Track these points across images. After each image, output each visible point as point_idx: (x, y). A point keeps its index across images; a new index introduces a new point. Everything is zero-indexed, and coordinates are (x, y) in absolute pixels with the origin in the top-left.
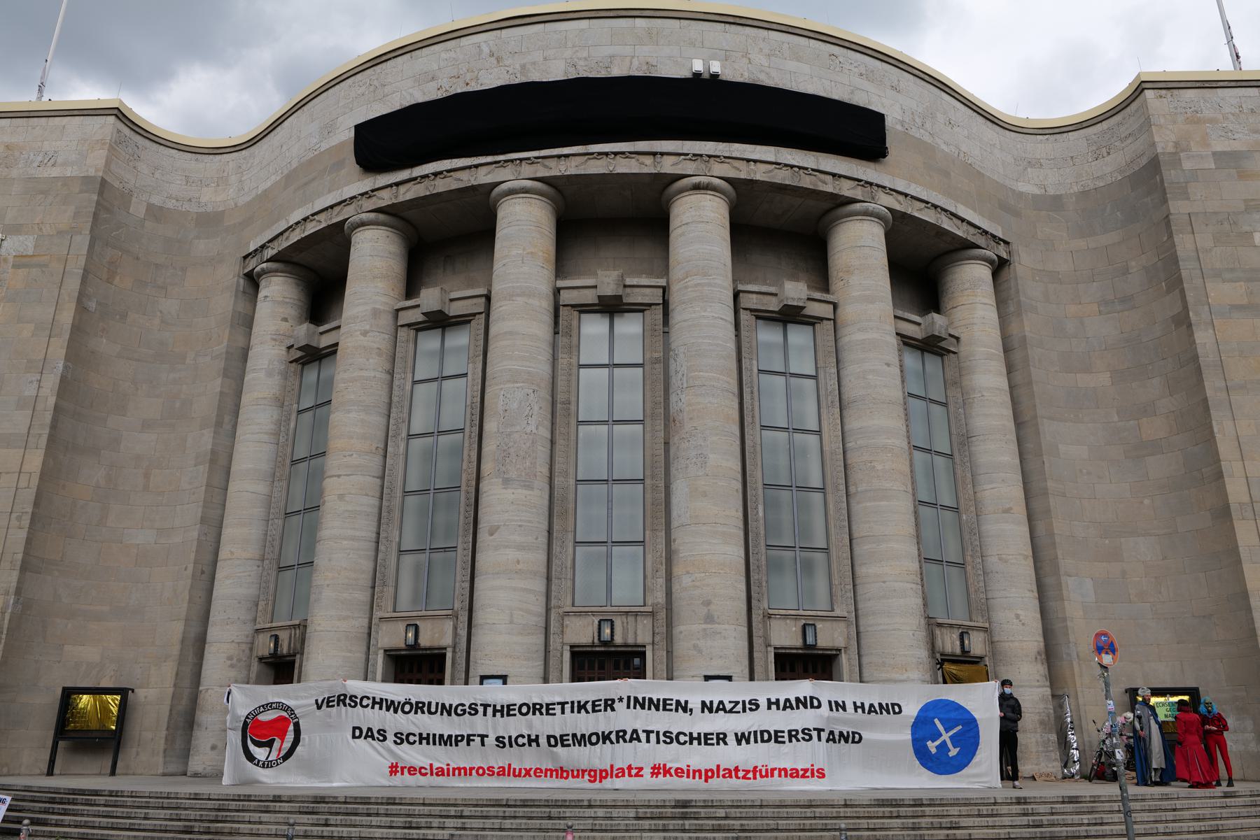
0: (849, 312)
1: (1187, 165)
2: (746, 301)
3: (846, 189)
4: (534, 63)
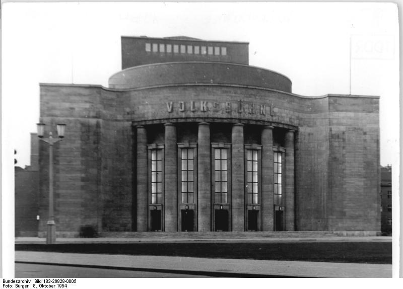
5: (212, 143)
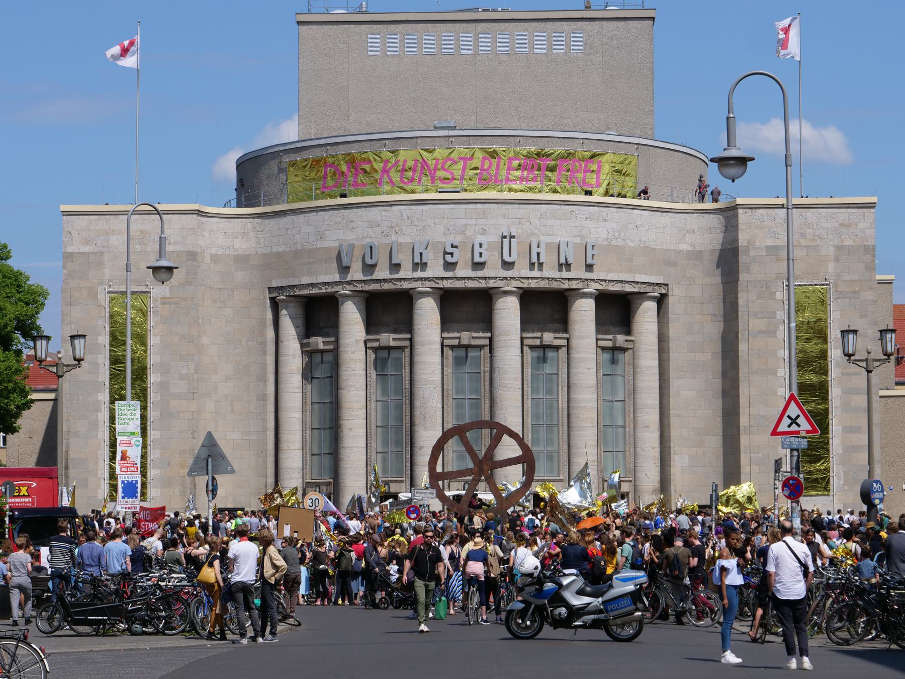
0: (574, 342)
1: (752, 253)
2: (526, 342)
3: (574, 285)
4: (429, 226)
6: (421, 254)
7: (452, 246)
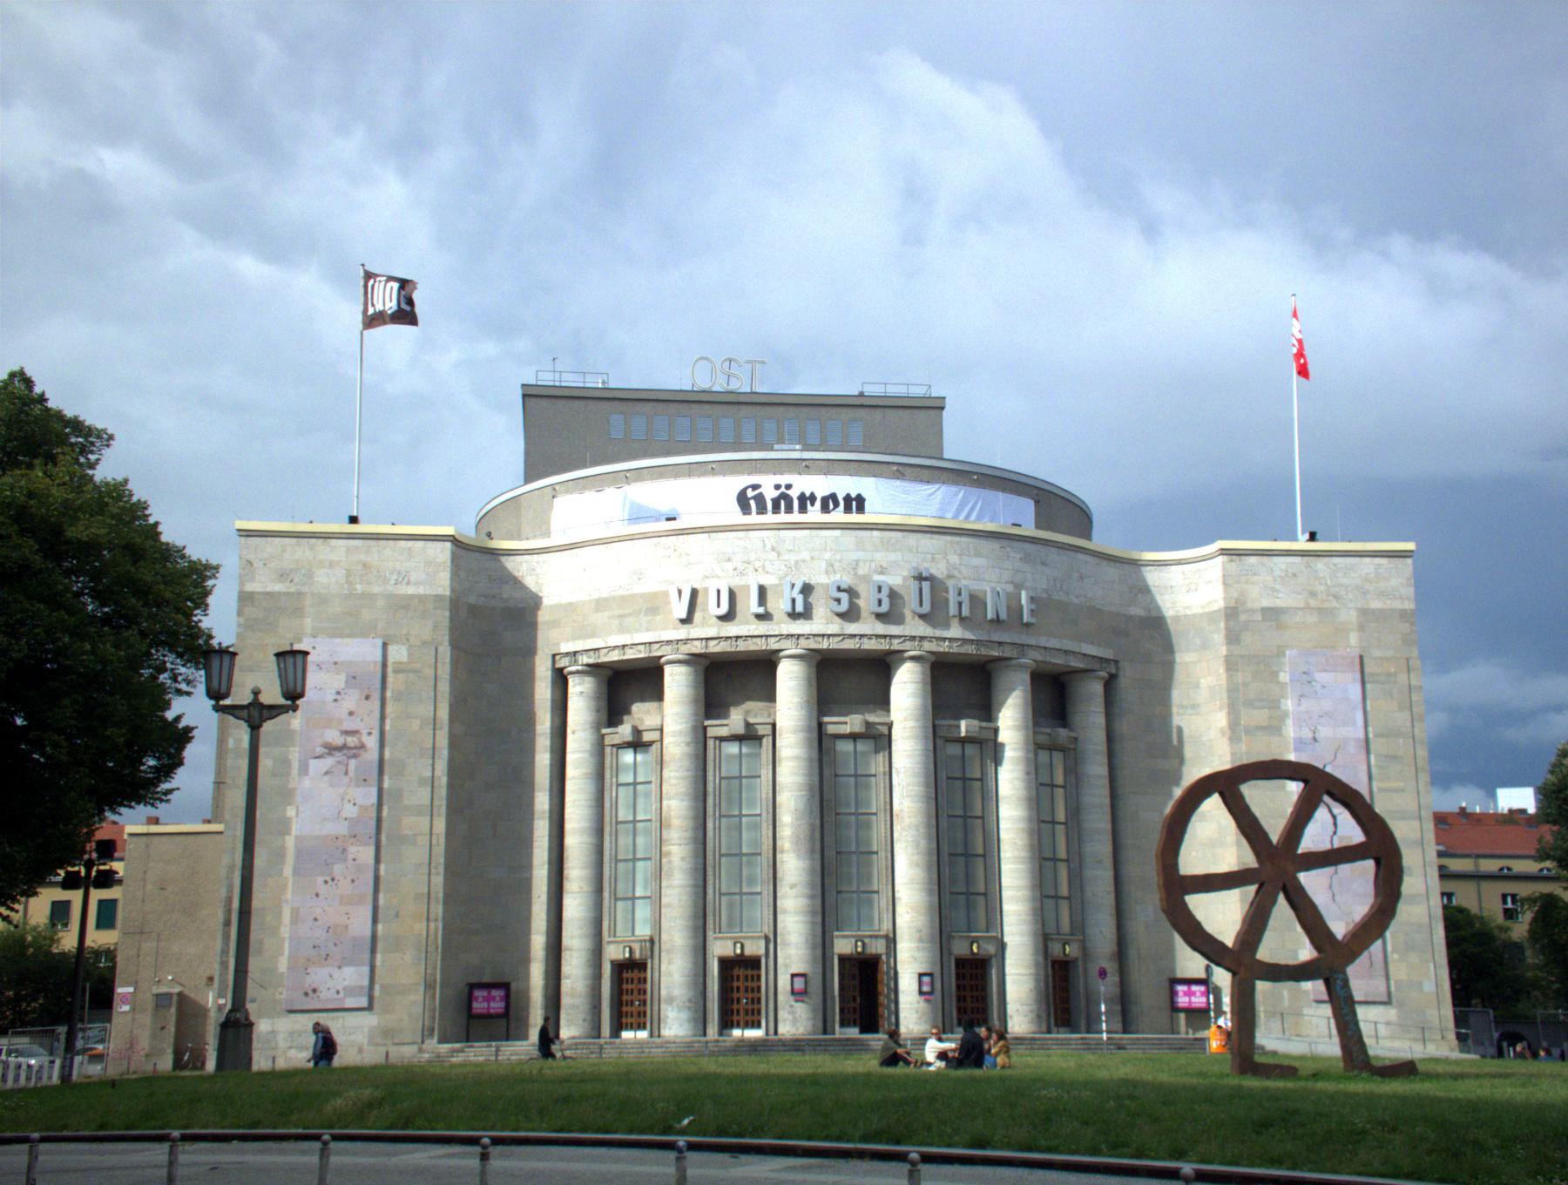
1: (1243, 617)
2: (940, 733)
3: (1008, 652)
5: (826, 719)
6: (794, 601)
7: (839, 589)
